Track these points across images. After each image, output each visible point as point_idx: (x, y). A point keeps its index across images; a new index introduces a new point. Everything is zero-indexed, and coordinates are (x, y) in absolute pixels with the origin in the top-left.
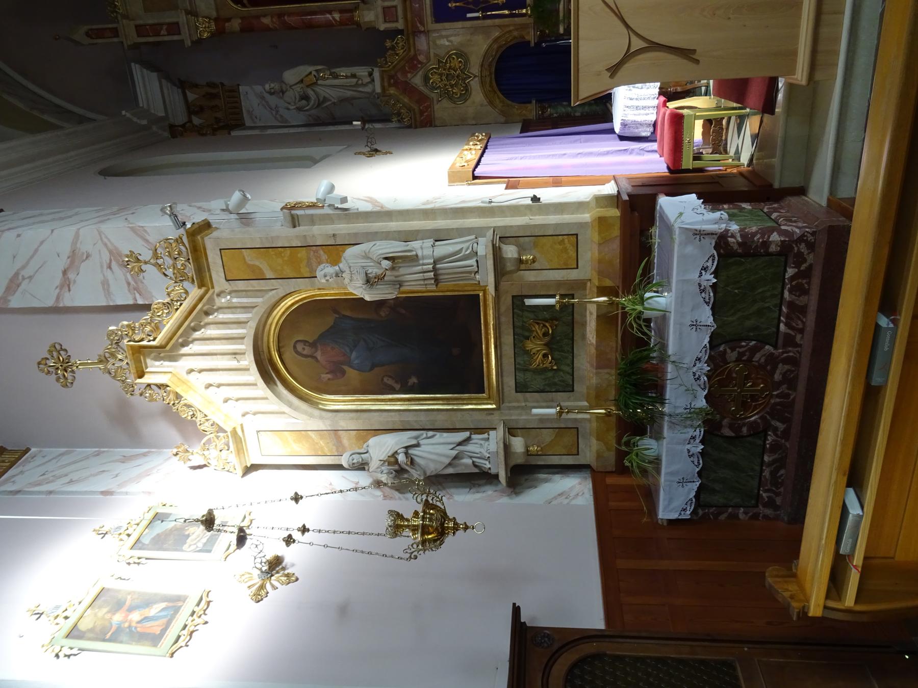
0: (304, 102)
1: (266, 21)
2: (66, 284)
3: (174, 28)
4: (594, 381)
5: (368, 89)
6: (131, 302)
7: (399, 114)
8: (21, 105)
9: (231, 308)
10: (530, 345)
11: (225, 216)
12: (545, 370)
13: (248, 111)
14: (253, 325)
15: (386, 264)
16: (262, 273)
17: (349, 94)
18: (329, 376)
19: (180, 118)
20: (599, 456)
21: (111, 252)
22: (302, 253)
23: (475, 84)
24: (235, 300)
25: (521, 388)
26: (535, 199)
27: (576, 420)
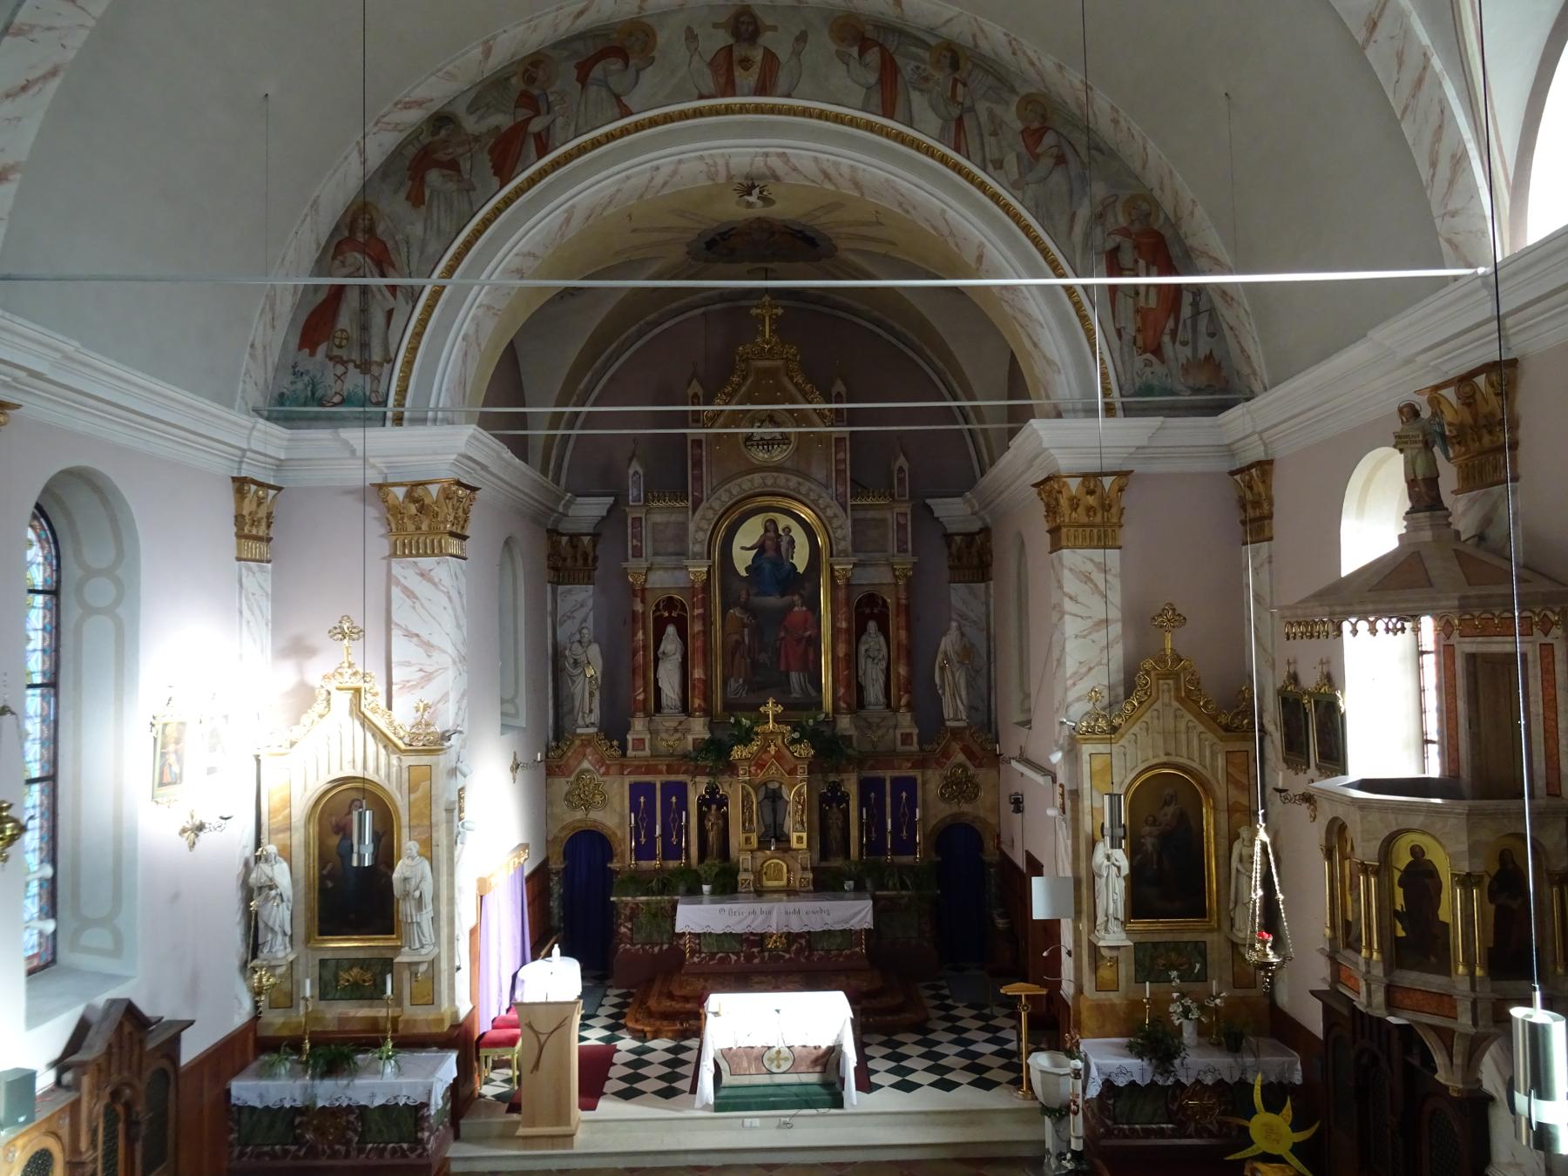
0: (572, 661)
1: (640, 635)
2: (410, 635)
3: (638, 553)
4: (328, 1016)
5: (580, 722)
6: (394, 680)
7: (558, 747)
8: (582, 386)
9: (389, 765)
10: (355, 971)
11: (454, 758)
12: (337, 981)
13: (570, 590)
14: (376, 779)
15: (417, 894)
16: (415, 792)
17: (577, 704)
18: (334, 823)
19: (566, 526)
20: (269, 1025)
21: (431, 673)
22: (426, 822)
23: (579, 815)
24: (395, 769)
25: (323, 963)
26: (459, 969)
27: (298, 1006)
